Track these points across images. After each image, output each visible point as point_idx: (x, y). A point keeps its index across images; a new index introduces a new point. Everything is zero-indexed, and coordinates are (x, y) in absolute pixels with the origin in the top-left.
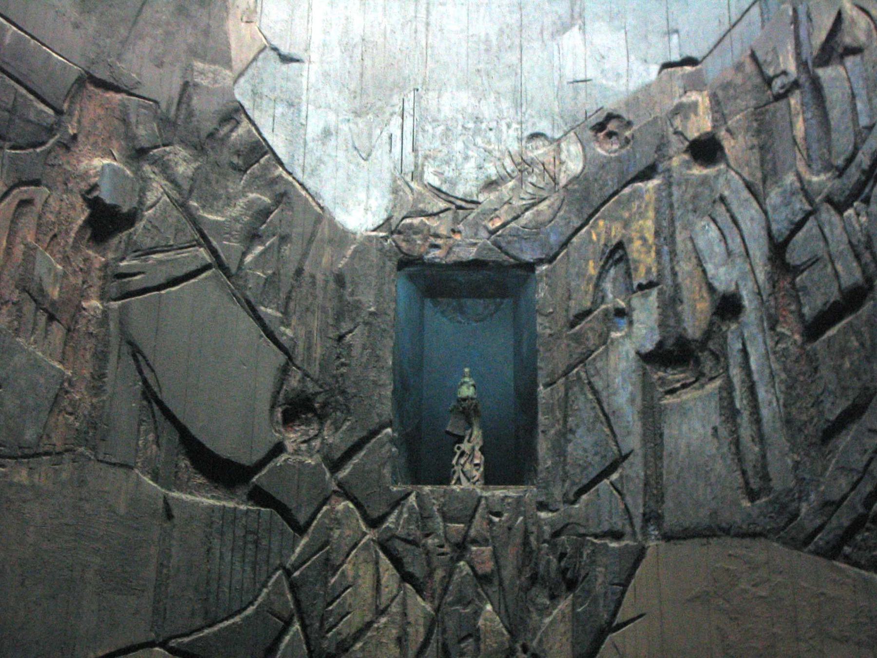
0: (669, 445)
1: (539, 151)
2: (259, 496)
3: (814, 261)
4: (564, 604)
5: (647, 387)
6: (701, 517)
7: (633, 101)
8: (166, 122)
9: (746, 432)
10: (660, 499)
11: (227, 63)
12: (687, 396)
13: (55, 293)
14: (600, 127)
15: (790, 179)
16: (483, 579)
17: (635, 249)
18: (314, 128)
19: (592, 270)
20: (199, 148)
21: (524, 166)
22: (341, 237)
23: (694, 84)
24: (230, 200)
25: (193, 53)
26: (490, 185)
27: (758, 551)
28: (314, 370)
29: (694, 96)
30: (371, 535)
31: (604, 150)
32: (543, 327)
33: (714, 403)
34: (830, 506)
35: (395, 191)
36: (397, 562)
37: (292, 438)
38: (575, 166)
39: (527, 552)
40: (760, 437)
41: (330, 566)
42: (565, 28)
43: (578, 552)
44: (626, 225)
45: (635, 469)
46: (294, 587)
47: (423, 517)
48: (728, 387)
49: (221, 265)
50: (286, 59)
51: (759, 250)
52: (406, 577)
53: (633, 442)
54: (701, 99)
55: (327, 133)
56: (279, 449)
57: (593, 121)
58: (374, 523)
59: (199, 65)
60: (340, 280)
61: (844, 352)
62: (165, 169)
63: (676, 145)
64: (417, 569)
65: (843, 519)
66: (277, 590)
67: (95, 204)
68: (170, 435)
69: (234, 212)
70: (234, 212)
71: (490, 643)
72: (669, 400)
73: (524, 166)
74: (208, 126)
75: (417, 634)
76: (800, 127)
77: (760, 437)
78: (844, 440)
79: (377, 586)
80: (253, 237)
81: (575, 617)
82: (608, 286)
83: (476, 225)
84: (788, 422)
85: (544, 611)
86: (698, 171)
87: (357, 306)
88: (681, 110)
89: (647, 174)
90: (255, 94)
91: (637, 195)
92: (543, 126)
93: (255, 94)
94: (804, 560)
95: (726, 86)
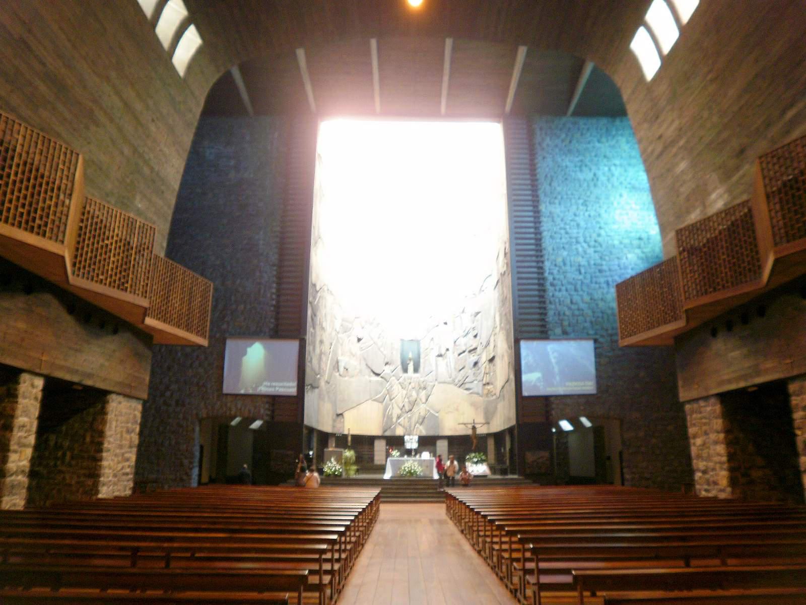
2: (382, 377)
3: (459, 345)
4: (424, 391)
6: (442, 380)
30: (397, 382)
32: (422, 350)
34: (459, 381)
36: (401, 386)
39: (419, 385)
41: (392, 387)
46: (388, 390)
47: (405, 379)
53: (434, 368)
64: (404, 387)
65: (461, 383)
68: (370, 370)
79: (398, 390)
81: (426, 394)
84: (455, 368)
94: (456, 388)
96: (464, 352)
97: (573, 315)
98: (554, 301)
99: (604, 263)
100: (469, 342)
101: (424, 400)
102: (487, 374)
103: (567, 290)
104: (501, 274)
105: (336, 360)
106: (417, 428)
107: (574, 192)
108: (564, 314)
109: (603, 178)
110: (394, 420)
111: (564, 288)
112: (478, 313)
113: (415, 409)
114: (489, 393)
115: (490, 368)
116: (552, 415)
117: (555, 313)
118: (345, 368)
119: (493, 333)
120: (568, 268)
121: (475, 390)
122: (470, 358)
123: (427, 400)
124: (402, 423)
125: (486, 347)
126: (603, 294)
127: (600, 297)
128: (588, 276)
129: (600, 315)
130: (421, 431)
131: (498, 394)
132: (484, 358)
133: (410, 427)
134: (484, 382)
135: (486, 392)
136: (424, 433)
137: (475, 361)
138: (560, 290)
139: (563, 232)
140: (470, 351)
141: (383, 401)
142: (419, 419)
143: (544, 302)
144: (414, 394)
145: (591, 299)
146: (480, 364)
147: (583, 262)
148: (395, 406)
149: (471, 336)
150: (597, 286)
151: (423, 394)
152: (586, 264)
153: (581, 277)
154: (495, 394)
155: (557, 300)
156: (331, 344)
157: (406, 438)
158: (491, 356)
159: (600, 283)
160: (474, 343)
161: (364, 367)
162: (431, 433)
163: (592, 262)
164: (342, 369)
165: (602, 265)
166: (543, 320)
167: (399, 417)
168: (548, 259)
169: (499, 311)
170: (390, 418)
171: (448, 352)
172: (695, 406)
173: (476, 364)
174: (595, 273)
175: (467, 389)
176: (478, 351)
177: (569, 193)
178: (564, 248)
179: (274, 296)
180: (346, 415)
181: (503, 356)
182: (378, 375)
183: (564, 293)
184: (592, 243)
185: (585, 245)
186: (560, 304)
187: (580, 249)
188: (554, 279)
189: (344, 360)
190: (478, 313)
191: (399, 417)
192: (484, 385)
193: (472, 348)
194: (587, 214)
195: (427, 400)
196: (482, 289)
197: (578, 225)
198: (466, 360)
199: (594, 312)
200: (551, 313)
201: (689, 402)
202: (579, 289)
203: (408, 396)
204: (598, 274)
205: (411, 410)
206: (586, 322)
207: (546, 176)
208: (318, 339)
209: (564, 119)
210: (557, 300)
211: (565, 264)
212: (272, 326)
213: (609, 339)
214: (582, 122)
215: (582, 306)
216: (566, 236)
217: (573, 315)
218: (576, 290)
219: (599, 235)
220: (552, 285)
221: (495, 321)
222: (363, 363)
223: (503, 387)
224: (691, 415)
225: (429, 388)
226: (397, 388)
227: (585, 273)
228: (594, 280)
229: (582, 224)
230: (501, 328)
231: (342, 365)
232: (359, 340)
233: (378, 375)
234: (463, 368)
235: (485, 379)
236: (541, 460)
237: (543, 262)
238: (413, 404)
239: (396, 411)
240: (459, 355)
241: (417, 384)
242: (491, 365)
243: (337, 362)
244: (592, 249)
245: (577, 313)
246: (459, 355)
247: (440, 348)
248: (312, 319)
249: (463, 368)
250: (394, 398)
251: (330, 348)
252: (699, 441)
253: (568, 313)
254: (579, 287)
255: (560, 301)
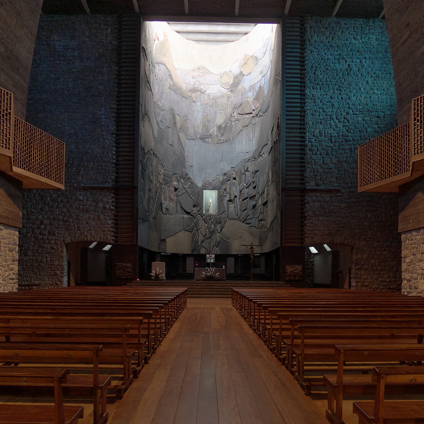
0: (229, 210)
1: (218, 177)
2: (191, 215)
4: (219, 225)
5: (228, 204)
7: (228, 172)
8: (180, 177)
9: (236, 210)
10: (228, 215)
11: (186, 168)
12: (231, 205)
13: (172, 198)
14: (224, 174)
15: (242, 184)
16: (212, 222)
17: (227, 189)
18: (195, 175)
19: (223, 191)
20: (184, 179)
21: (217, 178)
22: (198, 187)
23: (234, 171)
24: (187, 184)
25: (183, 168)
26: (213, 181)
27: (237, 221)
28: (196, 202)
29: (234, 172)
30: (202, 218)
31: (225, 177)
33: (234, 207)
34: (243, 218)
35: (203, 182)
36: (204, 221)
37: (194, 209)
38: (222, 179)
39: (216, 220)
40: (237, 210)
42: (221, 162)
43: (221, 220)
44: (226, 186)
45: (226, 212)
47: (207, 216)
48: (235, 205)
49: (187, 192)
50: (192, 167)
51: (239, 191)
52: (205, 222)
53: (226, 210)
54: (234, 173)
55: (196, 175)
56: (193, 210)
57: (224, 174)
58: (202, 217)
59: (183, 169)
60: (198, 192)
61: (245, 203)
62: (181, 182)
63: (232, 178)
65: (244, 219)
66: (193, 224)
67: (175, 188)
68: (183, 210)
69: (187, 186)
70: (187, 186)
71: (213, 229)
72: (230, 206)
73: (217, 178)
74: (185, 176)
75: (206, 228)
76: (243, 179)
77: (237, 210)
78: (245, 212)
80: (190, 188)
82: (224, 193)
83: (211, 185)
85: (218, 226)
86: (234, 181)
87: (200, 195)
88: (233, 174)
89: (229, 180)
90: (189, 171)
91: (228, 183)
92: (218, 174)
93: (189, 171)
95: (237, 172)
96: (247, 198)
97: (324, 172)
98: (311, 162)
99: (349, 134)
100: (250, 191)
101: (219, 231)
102: (261, 213)
103: (320, 155)
104: (274, 142)
105: (160, 202)
106: (215, 249)
107: (332, 80)
108: (318, 172)
109: (355, 69)
110: (200, 243)
111: (318, 153)
112: (257, 171)
113: (214, 237)
114: (263, 225)
115: (263, 209)
116: (305, 241)
117: (311, 170)
118: (166, 208)
119: (267, 185)
120: (323, 138)
121: (253, 224)
122: (250, 202)
123: (221, 231)
124: (205, 246)
125: (262, 195)
126: (347, 158)
127: (345, 159)
128: (337, 144)
129: (343, 172)
130: (217, 251)
131: (268, 227)
132: (260, 203)
133: (210, 249)
134: (260, 219)
135: (261, 225)
136: (219, 253)
137: (253, 204)
138: (316, 154)
139: (321, 110)
140: (250, 198)
141: (192, 231)
142: (216, 243)
143: (304, 163)
144: (213, 226)
145: (337, 161)
146: (257, 207)
147: (335, 134)
148: (200, 234)
149: (251, 187)
150: (343, 151)
151: (218, 227)
152: (336, 135)
153: (332, 145)
154: (267, 227)
155: (313, 161)
156: (157, 192)
157: (208, 256)
158: (265, 201)
159: (345, 149)
160: (253, 192)
161: (179, 208)
162: (224, 253)
163: (341, 134)
164: (164, 209)
165: (348, 136)
166: (302, 175)
167: (202, 242)
168: (308, 131)
169: (272, 170)
170: (197, 242)
171: (236, 199)
172: (409, 235)
173: (254, 206)
174: (342, 142)
175: (247, 224)
176: (256, 199)
177: (328, 80)
178: (321, 123)
179: (114, 157)
180: (168, 240)
181: (273, 200)
182: (188, 213)
183: (319, 156)
184: (342, 120)
185: (337, 121)
186: (315, 164)
187: (333, 124)
188: (312, 146)
189: (166, 204)
190: (257, 171)
191: (202, 242)
192: (260, 221)
193: (252, 196)
194: (340, 97)
195: (221, 231)
196: (261, 154)
197: (333, 105)
198: (248, 204)
199: (339, 171)
200: (308, 170)
201: (405, 232)
202: (330, 154)
203: (209, 228)
204: (344, 143)
205: (211, 237)
206: (333, 177)
207: (312, 67)
208: (147, 187)
209: (330, 20)
210: (313, 161)
211: (321, 135)
212: (114, 178)
213: (348, 190)
214: (343, 21)
215: (331, 166)
216: (323, 113)
217: (324, 172)
218: (327, 154)
219: (348, 113)
220: (311, 150)
221: (268, 176)
222: (179, 205)
223: (272, 222)
224: (405, 242)
225: (223, 223)
226: (201, 222)
227: (335, 142)
228: (341, 148)
229: (336, 105)
230: (273, 181)
231: (164, 206)
232: (176, 189)
233: (188, 213)
234: (246, 209)
235: (260, 216)
236: (296, 271)
237: (305, 133)
238: (212, 233)
239: (201, 238)
240: (243, 200)
241: (215, 220)
242: (265, 207)
243: (161, 204)
244: (342, 124)
245: (327, 170)
246: (243, 200)
247: (230, 195)
248: (142, 173)
249: (246, 209)
250: (199, 229)
251: (156, 195)
252: (408, 260)
253: (320, 170)
254: (329, 151)
255: (315, 162)
